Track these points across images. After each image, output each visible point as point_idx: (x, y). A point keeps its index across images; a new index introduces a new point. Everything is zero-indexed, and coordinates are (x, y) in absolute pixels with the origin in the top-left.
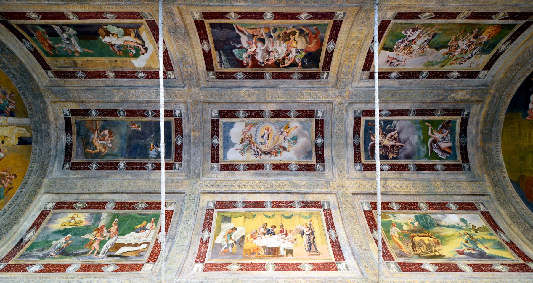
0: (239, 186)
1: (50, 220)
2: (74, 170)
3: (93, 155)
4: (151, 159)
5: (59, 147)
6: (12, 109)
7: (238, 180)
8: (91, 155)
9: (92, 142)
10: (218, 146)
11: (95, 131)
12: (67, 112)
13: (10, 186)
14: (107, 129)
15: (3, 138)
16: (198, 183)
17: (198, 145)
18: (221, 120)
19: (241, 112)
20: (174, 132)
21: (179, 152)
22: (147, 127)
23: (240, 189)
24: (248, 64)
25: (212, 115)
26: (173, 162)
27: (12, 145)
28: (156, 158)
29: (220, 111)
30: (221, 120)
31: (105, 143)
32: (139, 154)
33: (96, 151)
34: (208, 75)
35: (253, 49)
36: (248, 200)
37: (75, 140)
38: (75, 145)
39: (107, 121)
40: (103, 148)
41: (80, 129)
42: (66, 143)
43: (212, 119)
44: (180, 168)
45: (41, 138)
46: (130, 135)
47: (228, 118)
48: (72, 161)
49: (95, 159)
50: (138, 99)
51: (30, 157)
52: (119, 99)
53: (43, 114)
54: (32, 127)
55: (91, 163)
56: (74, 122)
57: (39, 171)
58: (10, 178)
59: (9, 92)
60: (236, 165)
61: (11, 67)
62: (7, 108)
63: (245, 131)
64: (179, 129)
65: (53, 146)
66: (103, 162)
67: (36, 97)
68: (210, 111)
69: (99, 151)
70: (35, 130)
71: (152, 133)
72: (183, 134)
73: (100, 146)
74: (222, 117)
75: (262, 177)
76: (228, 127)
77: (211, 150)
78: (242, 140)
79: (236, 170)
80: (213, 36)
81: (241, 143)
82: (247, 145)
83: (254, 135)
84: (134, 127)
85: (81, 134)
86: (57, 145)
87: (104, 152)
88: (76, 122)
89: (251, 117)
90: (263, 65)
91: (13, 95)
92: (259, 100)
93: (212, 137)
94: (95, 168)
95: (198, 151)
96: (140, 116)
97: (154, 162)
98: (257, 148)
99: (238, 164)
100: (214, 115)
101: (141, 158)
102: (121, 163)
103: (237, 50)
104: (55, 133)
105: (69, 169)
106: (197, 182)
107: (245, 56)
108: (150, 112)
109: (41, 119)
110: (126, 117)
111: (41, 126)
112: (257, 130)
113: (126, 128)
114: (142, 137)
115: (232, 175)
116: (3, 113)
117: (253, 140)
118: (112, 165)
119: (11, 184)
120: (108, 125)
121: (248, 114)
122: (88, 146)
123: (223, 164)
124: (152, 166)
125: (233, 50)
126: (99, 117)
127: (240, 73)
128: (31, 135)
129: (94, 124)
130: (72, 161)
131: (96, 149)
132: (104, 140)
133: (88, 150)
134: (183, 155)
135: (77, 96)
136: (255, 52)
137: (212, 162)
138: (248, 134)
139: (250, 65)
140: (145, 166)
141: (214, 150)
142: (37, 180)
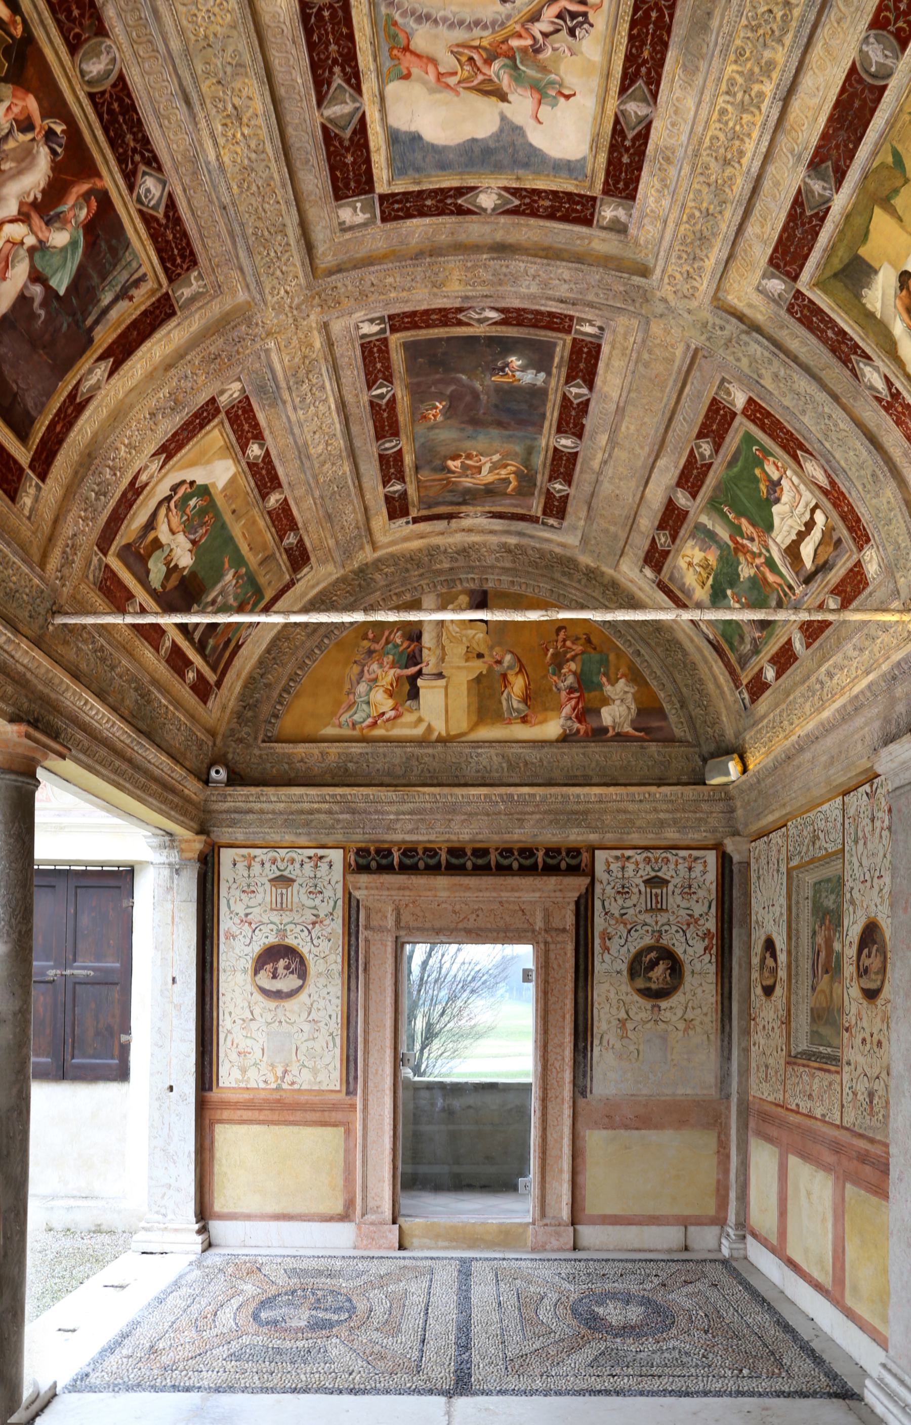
0: (726, 162)
1: (683, 592)
6: (403, 636)
7: (697, 154)
10: (515, 192)
13: (582, 641)
15: (470, 655)
16: (671, 297)
18: (381, 188)
19: (328, 112)
20: (447, 329)
23: (745, 161)
24: (86, 196)
25: (365, 225)
26: (569, 339)
27: (488, 638)
29: (338, 198)
30: (381, 188)
34: (193, 299)
35: (17, 231)
36: (814, 140)
43: (384, 220)
45: (471, 569)
46: (463, 422)
47: (368, 161)
49: (538, 483)
51: (519, 595)
53: (409, 566)
57: (557, 575)
58: (564, 641)
59: (366, 644)
60: (618, 131)
61: (308, 644)
62: (401, 649)
63: (432, 77)
65: (494, 539)
67: (368, 585)
68: (348, 236)
70: (451, 583)
74: (366, 184)
75: (715, 23)
76: (418, 156)
77: (532, 221)
78: (487, 93)
79: (644, 136)
80: (49, 393)
81: (503, 98)
82: (516, 67)
83: (460, 35)
89: (350, 58)
90: (59, 128)
91: (371, 636)
92: (247, 58)
93: (469, 212)
98: (535, 17)
99: (617, 122)
100: (361, 218)
103: (53, 283)
106: (664, 300)
107: (59, 238)
109: (422, 571)
111: (440, 572)
112: (428, 17)
114: (468, 398)
115: (668, 160)
116: (414, 656)
117: (486, 38)
119: (578, 639)
121: (338, 81)
123: (606, 183)
125: (62, 292)
127: (139, 201)
128: (462, 592)
130: (539, 514)
133: (509, 490)
136: (23, 217)
137: (587, 221)
138: (448, 62)
139: (85, 187)
141: (532, 208)
142: (579, 581)
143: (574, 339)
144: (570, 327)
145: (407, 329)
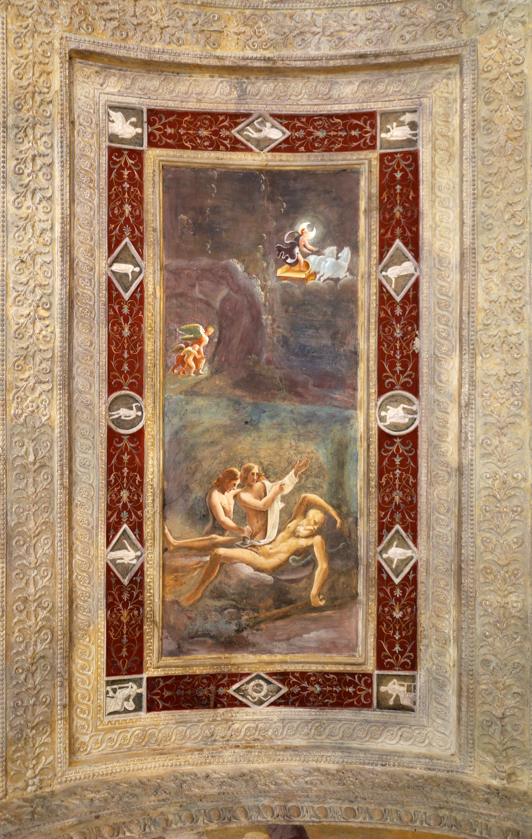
2: (414, 650)
3: (339, 563)
4: (362, 267)
5: (298, 741)
8: (340, 573)
9: (276, 570)
11: (216, 558)
12: (122, 693)
14: (208, 494)
17: (289, 22)
20: (219, 154)
21: (321, 134)
22: (197, 293)
28: (355, 249)
31: (278, 505)
32: (334, 337)
33: (319, 553)
37: (265, 657)
38: (288, 658)
39: (164, 492)
40: (305, 514)
41: (207, 634)
42: (274, 704)
44: (408, 118)
46: (236, 385)
48: (370, 667)
49: (362, 552)
50: (56, 300)
52: (56, 403)
54: (213, 826)
55: (380, 568)
56: (170, 660)
64: (203, 133)
66: (374, 510)
69: (318, 539)
71: (226, 269)
72: (232, 108)
73: (294, 534)
84: (195, 360)
85: (233, 627)
86: (286, 748)
87: (326, 512)
88: (171, 654)
94: (403, 545)
95: (320, 21)
96: (138, 322)
97: (375, 255)
101: (354, 327)
102: (382, 419)
104: (228, 754)
105: (413, 678)
108: (118, 267)
110: (148, 392)
113: (199, 402)
114: (245, 320)
118: (392, 463)
120: (186, 489)
122: (295, 590)
124: (399, 259)
126: (147, 530)
129: (180, 561)
130: (370, 667)
131: (307, 551)
132: (263, 514)
133: (314, 591)
134: (337, 108)
135: (42, 614)
140: (398, 299)
143: (382, 156)
144: (374, 138)
145: (167, 146)
